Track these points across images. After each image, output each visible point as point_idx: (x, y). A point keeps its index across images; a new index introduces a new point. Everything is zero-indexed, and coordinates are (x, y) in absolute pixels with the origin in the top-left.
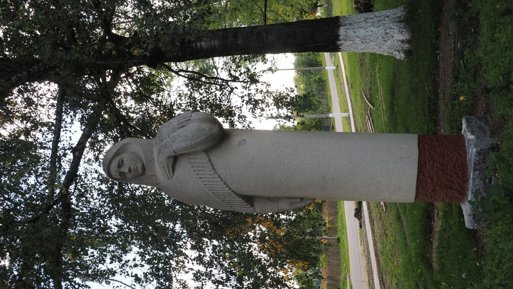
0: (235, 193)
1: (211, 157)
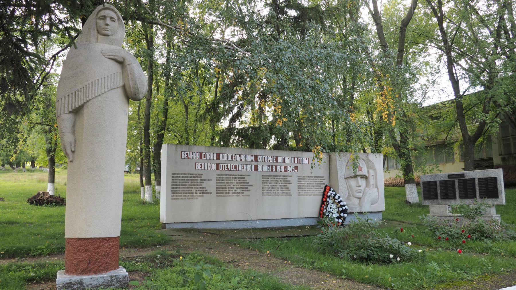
0: (88, 101)
1: (119, 89)
